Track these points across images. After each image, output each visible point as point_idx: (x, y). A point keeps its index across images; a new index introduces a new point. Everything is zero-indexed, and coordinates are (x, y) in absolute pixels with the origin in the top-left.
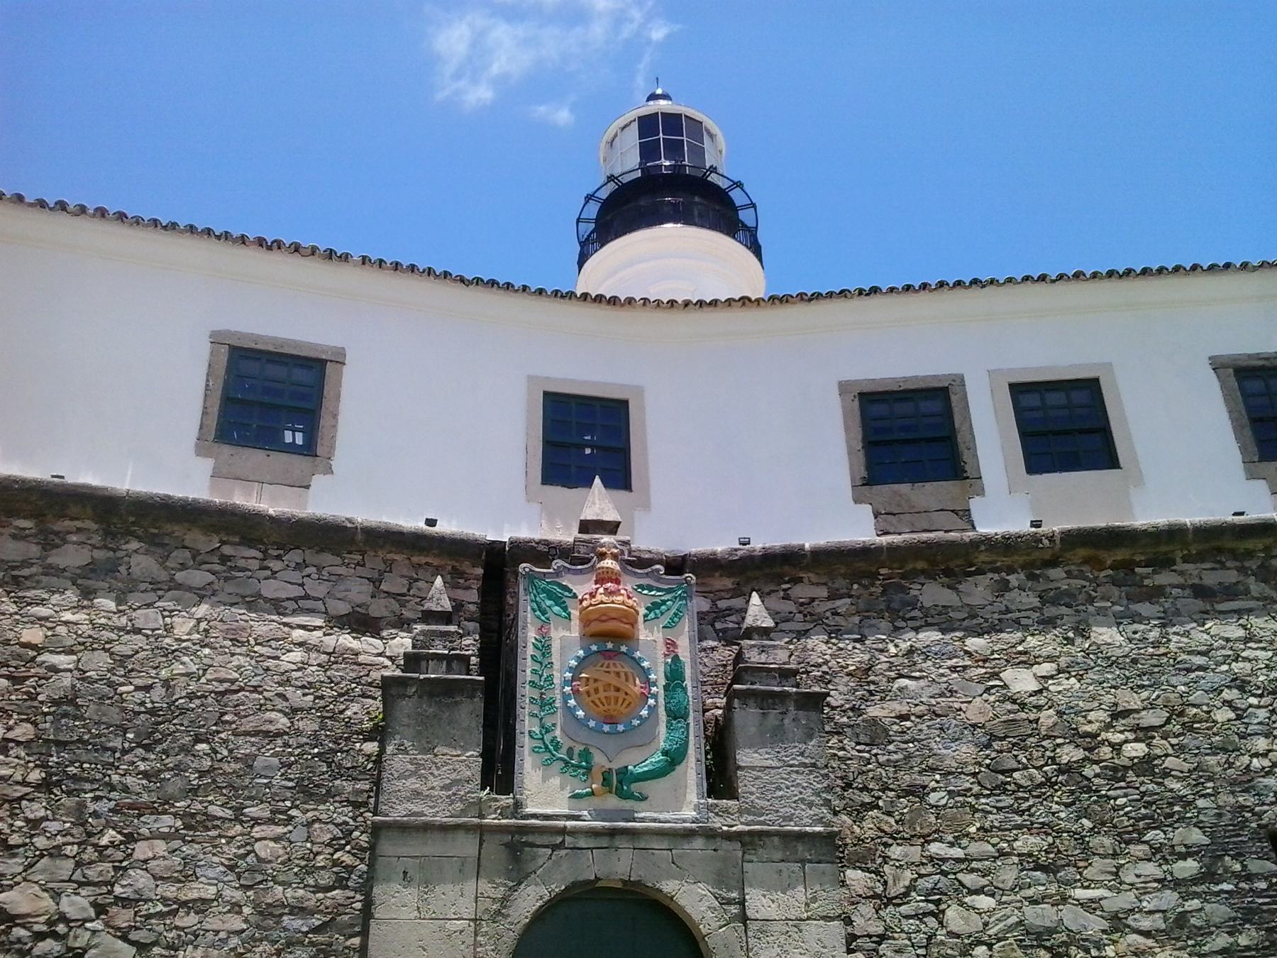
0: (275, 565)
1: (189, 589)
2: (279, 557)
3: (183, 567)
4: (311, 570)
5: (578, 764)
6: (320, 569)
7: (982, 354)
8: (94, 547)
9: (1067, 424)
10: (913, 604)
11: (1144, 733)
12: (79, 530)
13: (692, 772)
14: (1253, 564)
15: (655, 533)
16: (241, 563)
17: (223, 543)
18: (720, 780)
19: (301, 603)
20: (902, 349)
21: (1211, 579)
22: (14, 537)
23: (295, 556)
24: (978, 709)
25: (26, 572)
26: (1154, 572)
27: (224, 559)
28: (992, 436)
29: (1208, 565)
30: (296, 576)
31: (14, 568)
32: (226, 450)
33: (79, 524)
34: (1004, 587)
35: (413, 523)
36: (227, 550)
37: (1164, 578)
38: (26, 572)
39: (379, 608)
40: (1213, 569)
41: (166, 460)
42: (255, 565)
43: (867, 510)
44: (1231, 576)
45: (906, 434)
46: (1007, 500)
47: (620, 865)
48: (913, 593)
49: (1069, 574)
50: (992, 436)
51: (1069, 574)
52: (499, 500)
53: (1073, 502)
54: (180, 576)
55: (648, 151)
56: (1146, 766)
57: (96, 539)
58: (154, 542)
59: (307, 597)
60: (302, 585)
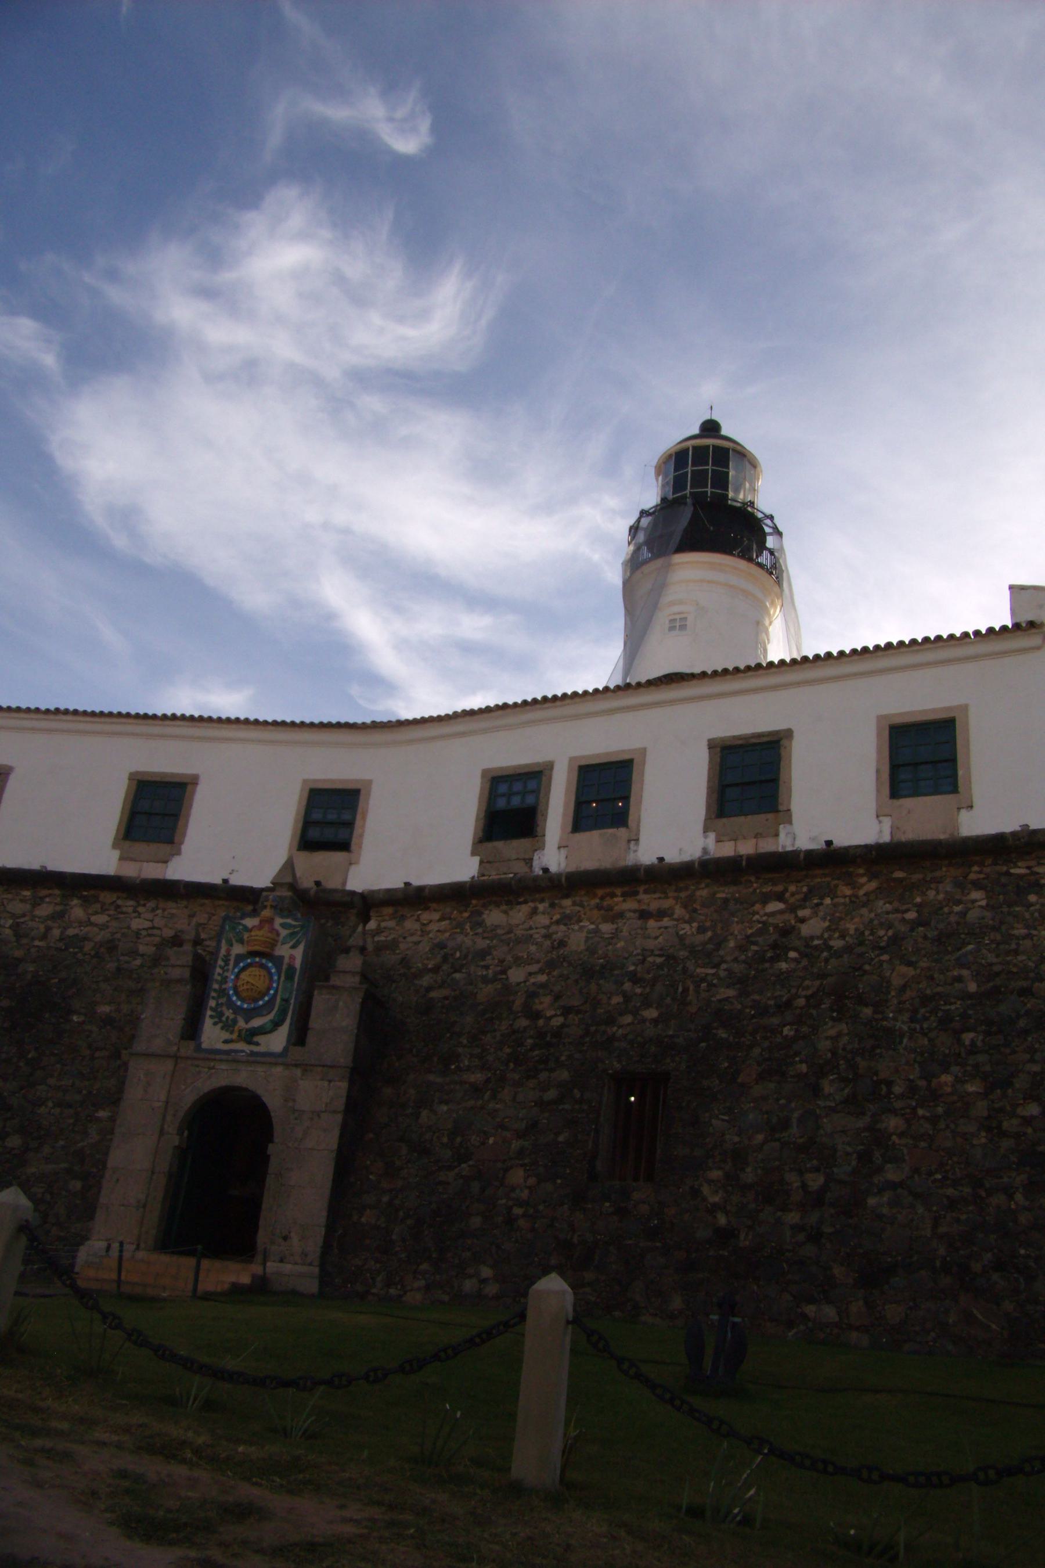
0: (141, 909)
1: (96, 925)
2: (144, 905)
3: (96, 913)
4: (159, 912)
5: (228, 1026)
6: (164, 910)
8: (56, 904)
10: (481, 924)
11: (567, 1011)
12: (50, 895)
13: (284, 1031)
14: (683, 895)
16: (124, 909)
17: (118, 898)
18: (300, 1036)
19: (150, 932)
21: (654, 906)
22: (21, 901)
23: (151, 904)
24: (486, 992)
25: (22, 920)
26: (624, 901)
27: (118, 907)
29: (657, 895)
30: (150, 916)
31: (18, 918)
32: (128, 844)
33: (50, 891)
34: (534, 912)
36: (119, 902)
37: (630, 904)
38: (22, 920)
40: (660, 898)
42: (130, 910)
43: (477, 859)
44: (667, 904)
46: (555, 851)
47: (242, 1078)
48: (485, 916)
49: (574, 904)
51: (574, 904)
53: (595, 851)
54: (93, 919)
56: (558, 1033)
57: (58, 900)
58: (86, 901)
59: (153, 928)
60: (152, 921)
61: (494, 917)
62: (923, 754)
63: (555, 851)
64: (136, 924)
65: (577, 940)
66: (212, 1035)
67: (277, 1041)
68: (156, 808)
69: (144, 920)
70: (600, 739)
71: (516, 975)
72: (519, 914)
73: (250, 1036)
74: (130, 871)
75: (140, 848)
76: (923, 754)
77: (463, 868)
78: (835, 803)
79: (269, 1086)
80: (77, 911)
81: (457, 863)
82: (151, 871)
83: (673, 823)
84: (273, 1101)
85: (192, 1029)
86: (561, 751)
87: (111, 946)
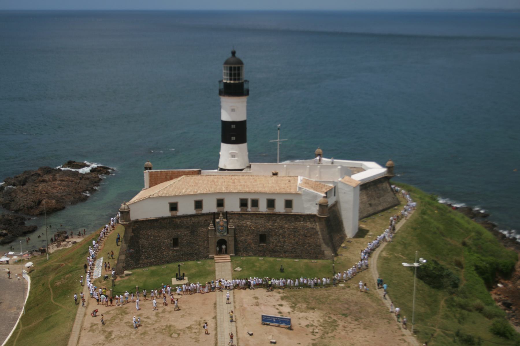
9: (255, 203)
20: (244, 197)
28: (249, 204)
39: (207, 219)
50: (249, 204)
62: (289, 204)
63: (250, 209)
64: (201, 219)
67: (226, 234)
68: (199, 204)
70: (254, 197)
74: (198, 212)
76: (289, 204)
78: (280, 208)
79: (226, 239)
80: (193, 219)
81: (237, 209)
82: (200, 212)
83: (263, 208)
86: (250, 198)
87: (199, 222)
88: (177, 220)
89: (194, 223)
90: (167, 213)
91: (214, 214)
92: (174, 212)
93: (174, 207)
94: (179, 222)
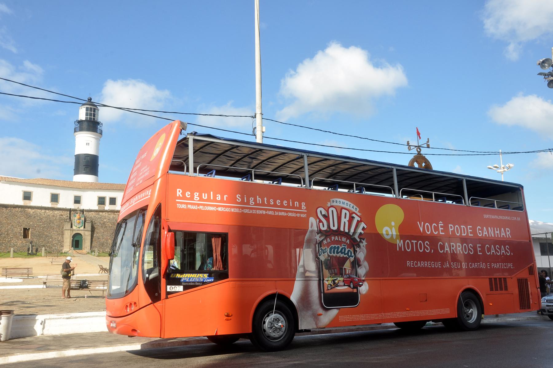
7: (108, 195)
9: (113, 201)
13: (83, 227)
15: (82, 208)
18: (84, 227)
20: (102, 194)
24: (102, 222)
28: (107, 201)
35: (64, 207)
41: (49, 204)
45: (101, 201)
46: (108, 207)
47: (79, 232)
50: (107, 201)
52: (71, 205)
53: (112, 207)
55: (87, 114)
61: (101, 213)
65: (111, 217)
66: (74, 228)
67: (82, 228)
69: (56, 212)
71: (105, 220)
72: (104, 213)
73: (79, 228)
74: (53, 206)
75: (54, 203)
77: (96, 207)
79: (82, 233)
84: (83, 234)
85: (71, 227)
88: (30, 210)
89: (49, 215)
90: (20, 202)
91: (70, 210)
92: (27, 201)
93: (27, 196)
94: (31, 212)
